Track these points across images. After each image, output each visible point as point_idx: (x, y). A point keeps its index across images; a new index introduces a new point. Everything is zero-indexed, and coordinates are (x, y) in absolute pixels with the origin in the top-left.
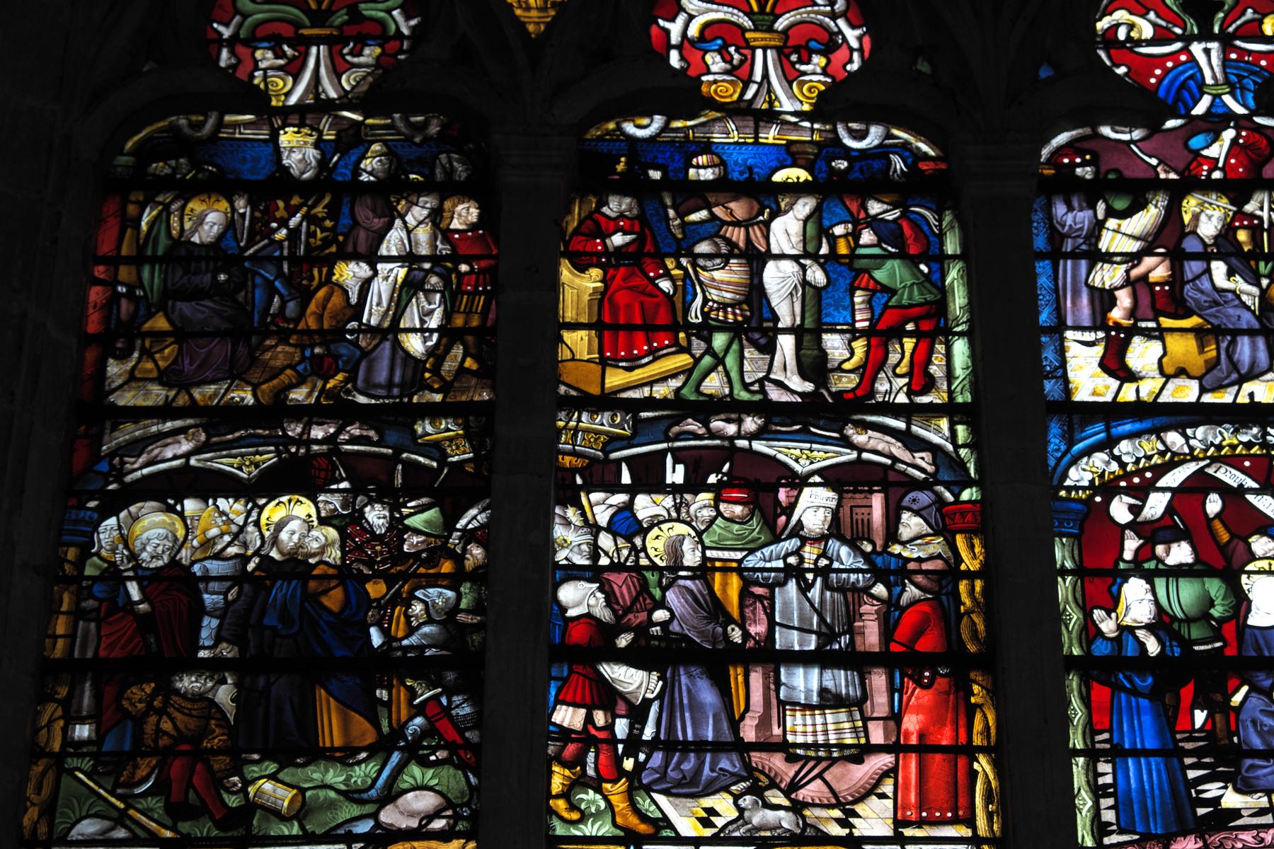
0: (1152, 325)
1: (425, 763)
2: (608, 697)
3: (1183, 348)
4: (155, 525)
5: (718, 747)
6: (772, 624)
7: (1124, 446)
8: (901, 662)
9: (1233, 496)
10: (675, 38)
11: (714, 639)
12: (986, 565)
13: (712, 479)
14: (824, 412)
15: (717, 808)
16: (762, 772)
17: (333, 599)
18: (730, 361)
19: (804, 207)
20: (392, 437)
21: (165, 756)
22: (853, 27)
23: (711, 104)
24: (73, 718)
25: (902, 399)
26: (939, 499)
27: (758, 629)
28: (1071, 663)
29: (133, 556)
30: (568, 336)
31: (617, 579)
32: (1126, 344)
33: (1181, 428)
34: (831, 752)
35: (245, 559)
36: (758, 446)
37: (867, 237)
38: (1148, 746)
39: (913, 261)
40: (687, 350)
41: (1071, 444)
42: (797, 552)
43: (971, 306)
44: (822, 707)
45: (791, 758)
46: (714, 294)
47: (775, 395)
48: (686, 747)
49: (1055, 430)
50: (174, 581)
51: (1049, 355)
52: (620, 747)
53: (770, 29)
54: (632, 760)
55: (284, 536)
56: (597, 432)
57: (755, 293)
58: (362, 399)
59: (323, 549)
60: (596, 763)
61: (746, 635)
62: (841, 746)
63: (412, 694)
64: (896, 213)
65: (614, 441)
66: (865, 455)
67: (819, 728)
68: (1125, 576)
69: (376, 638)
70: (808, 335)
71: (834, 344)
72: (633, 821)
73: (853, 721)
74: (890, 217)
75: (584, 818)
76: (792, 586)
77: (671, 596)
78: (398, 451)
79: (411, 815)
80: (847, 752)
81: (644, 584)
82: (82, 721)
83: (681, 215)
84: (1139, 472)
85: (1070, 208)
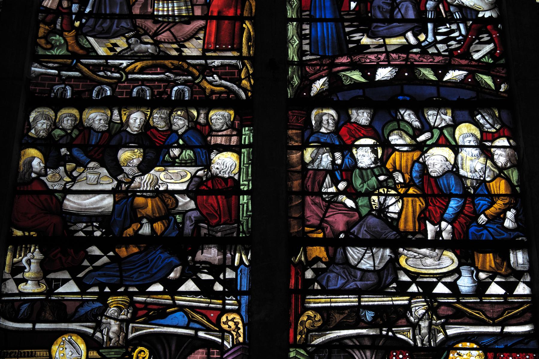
5: (121, 17)
15: (118, 43)
16: (141, 28)
34: (176, 19)
38: (327, 17)
45: (156, 22)
48: (105, 17)
52: (74, 16)
54: (79, 22)
60: (61, 23)
62: (180, 16)
67: (170, 9)
72: (77, 49)
73: (187, 6)
75: (53, 47)
80: (183, 20)
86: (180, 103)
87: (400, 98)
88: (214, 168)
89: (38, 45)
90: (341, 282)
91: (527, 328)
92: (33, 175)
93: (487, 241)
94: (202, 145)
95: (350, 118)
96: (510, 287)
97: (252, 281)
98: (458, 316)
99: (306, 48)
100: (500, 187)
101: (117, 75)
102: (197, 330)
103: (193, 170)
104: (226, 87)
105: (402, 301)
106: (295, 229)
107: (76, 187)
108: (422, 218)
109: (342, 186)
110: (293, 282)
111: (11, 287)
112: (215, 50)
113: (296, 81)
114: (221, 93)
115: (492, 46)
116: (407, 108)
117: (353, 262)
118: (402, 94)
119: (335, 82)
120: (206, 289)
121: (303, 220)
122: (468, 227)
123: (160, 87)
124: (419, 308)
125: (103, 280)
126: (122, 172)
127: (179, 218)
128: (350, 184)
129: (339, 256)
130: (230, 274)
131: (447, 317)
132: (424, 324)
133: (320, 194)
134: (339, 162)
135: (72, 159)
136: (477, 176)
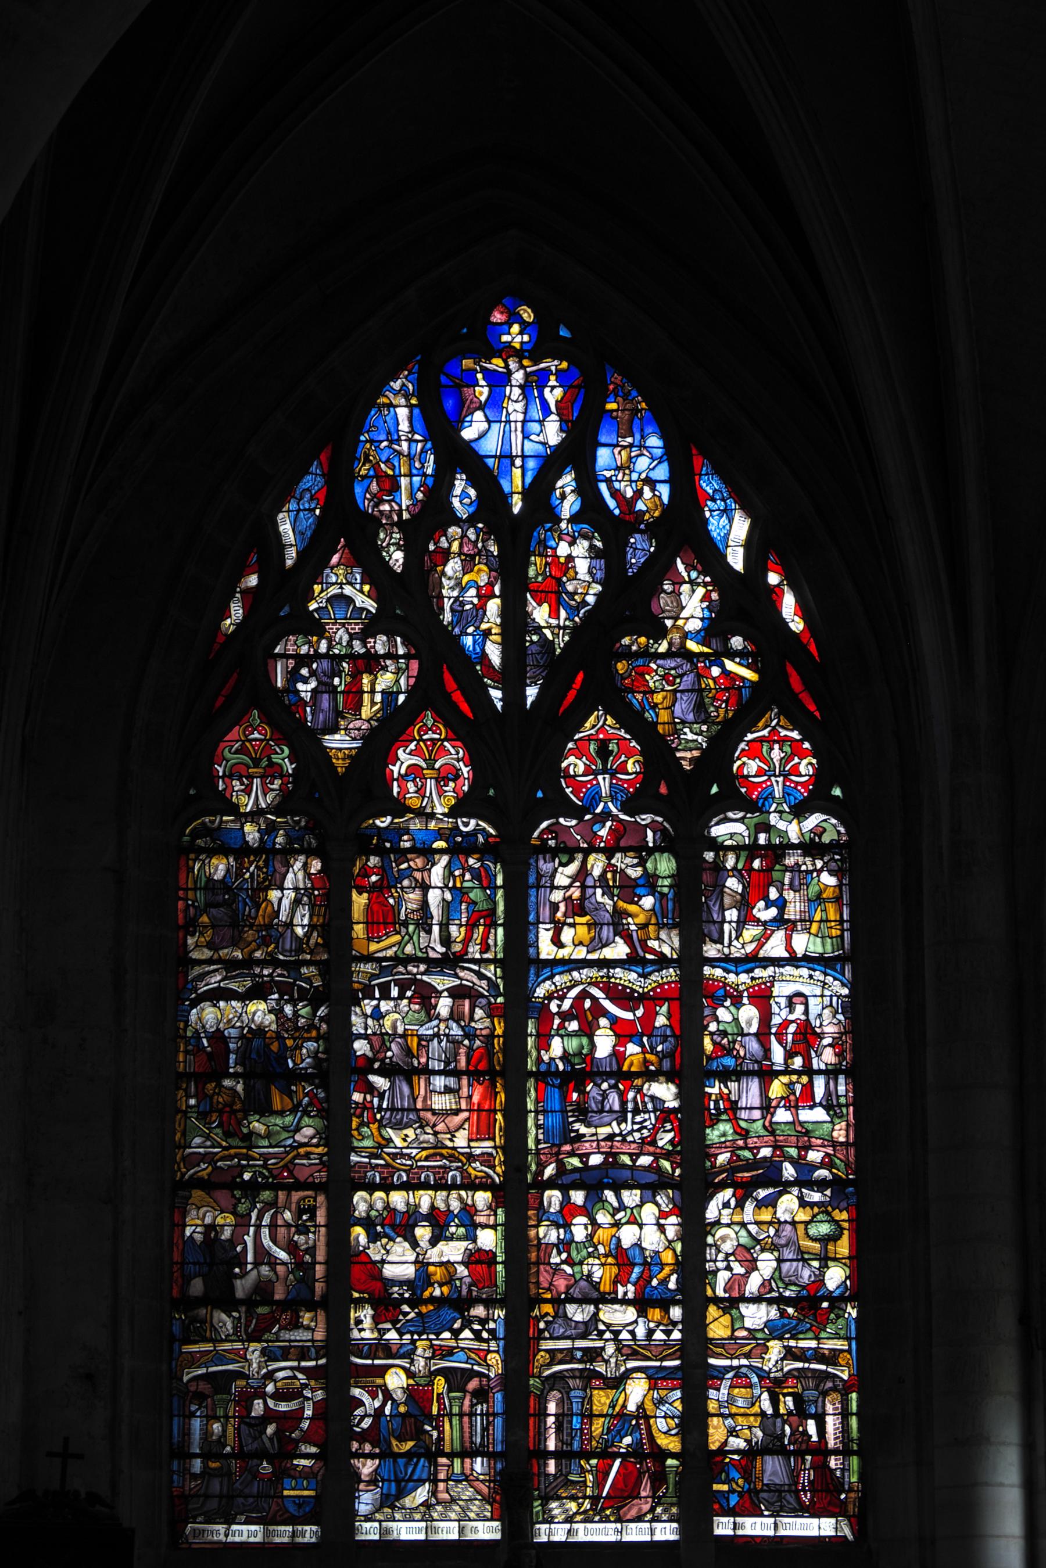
0: (570, 920)
1: (310, 1117)
2: (370, 1089)
3: (582, 931)
4: (210, 1013)
5: (409, 1110)
6: (428, 1058)
7: (557, 978)
8: (473, 1074)
9: (595, 1000)
10: (396, 775)
11: (407, 1064)
12: (504, 1032)
13: (409, 994)
14: (450, 962)
17: (275, 1047)
18: (415, 938)
19: (445, 860)
20: (292, 974)
21: (221, 1112)
22: (466, 766)
23: (410, 810)
24: (189, 1096)
25: (477, 956)
26: (489, 1002)
27: (423, 1060)
28: (531, 1074)
29: (204, 1027)
30: (356, 927)
31: (374, 1038)
32: (561, 929)
33: (578, 969)
35: (242, 1028)
36: (425, 978)
37: (468, 876)
39: (483, 888)
40: (399, 933)
41: (538, 977)
42: (438, 1026)
43: (506, 911)
44: (444, 1093)
46: (409, 906)
47: (432, 955)
48: (398, 1110)
49: (532, 971)
50: (218, 1037)
51: (532, 936)
53: (433, 769)
55: (256, 1018)
56: (367, 973)
57: (425, 904)
58: (281, 957)
59: (270, 1025)
61: (419, 1063)
62: (451, 1110)
63: (304, 1089)
64: (479, 864)
65: (374, 977)
66: (464, 982)
68: (553, 1036)
69: (291, 1065)
70: (444, 926)
71: (454, 930)
72: (380, 1139)
74: (476, 866)
75: (363, 1138)
76: (436, 1040)
77: (393, 1045)
78: (295, 981)
79: (306, 1137)
81: (383, 1042)
82: (192, 1097)
83: (397, 866)
84: (562, 990)
85: (545, 862)
86: (454, 1187)
87: (605, 1180)
88: (479, 1241)
89: (353, 1136)
90: (562, 1330)
91: (677, 1362)
92: (361, 1248)
93: (657, 1299)
94: (472, 1228)
95: (570, 1199)
96: (668, 1333)
97: (506, 1330)
98: (634, 1354)
99: (541, 1137)
100: (668, 1257)
101: (409, 1162)
102: (473, 1365)
103: (465, 1244)
104: (485, 1172)
105: (599, 1344)
106: (533, 1291)
107: (390, 1258)
108: (615, 1282)
109: (564, 1256)
110: (531, 1331)
111: (355, 1334)
112: (477, 1140)
113: (533, 1167)
114: (482, 1178)
115: (672, 1134)
116: (610, 1189)
117: (570, 1315)
118: (607, 1177)
119: (561, 1166)
120: (477, 1335)
121: (538, 1284)
122: (645, 1288)
123: (439, 1173)
124: (610, 1349)
125: (412, 1329)
126: (418, 1245)
127: (458, 1283)
128: (569, 1255)
129: (561, 1311)
130: (492, 1325)
131: (627, 1355)
132: (613, 1360)
133: (549, 1264)
134: (562, 1237)
135: (386, 1236)
136: (653, 1248)
